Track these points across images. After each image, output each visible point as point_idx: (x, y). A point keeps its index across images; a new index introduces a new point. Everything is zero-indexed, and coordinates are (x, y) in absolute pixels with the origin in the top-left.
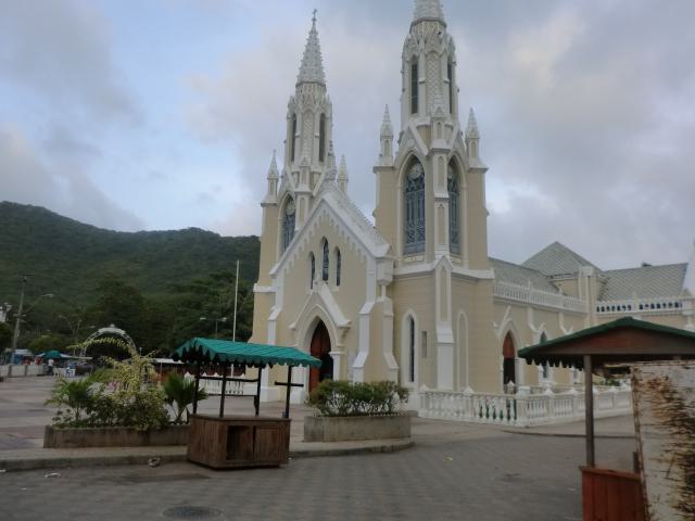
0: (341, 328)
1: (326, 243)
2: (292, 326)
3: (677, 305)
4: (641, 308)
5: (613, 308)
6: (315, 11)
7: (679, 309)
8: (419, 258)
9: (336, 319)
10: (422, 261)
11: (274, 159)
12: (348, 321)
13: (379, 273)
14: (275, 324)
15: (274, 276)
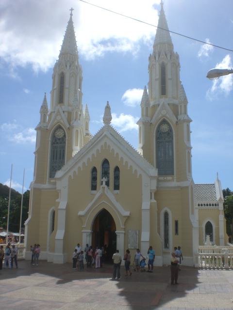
0: (125, 217)
1: (106, 162)
2: (81, 213)
3: (216, 205)
4: (199, 205)
5: (204, 204)
6: (72, 10)
7: (217, 207)
8: (169, 178)
9: (119, 211)
10: (173, 180)
11: (45, 96)
12: (129, 212)
13: (149, 186)
14: (64, 212)
15: (60, 179)
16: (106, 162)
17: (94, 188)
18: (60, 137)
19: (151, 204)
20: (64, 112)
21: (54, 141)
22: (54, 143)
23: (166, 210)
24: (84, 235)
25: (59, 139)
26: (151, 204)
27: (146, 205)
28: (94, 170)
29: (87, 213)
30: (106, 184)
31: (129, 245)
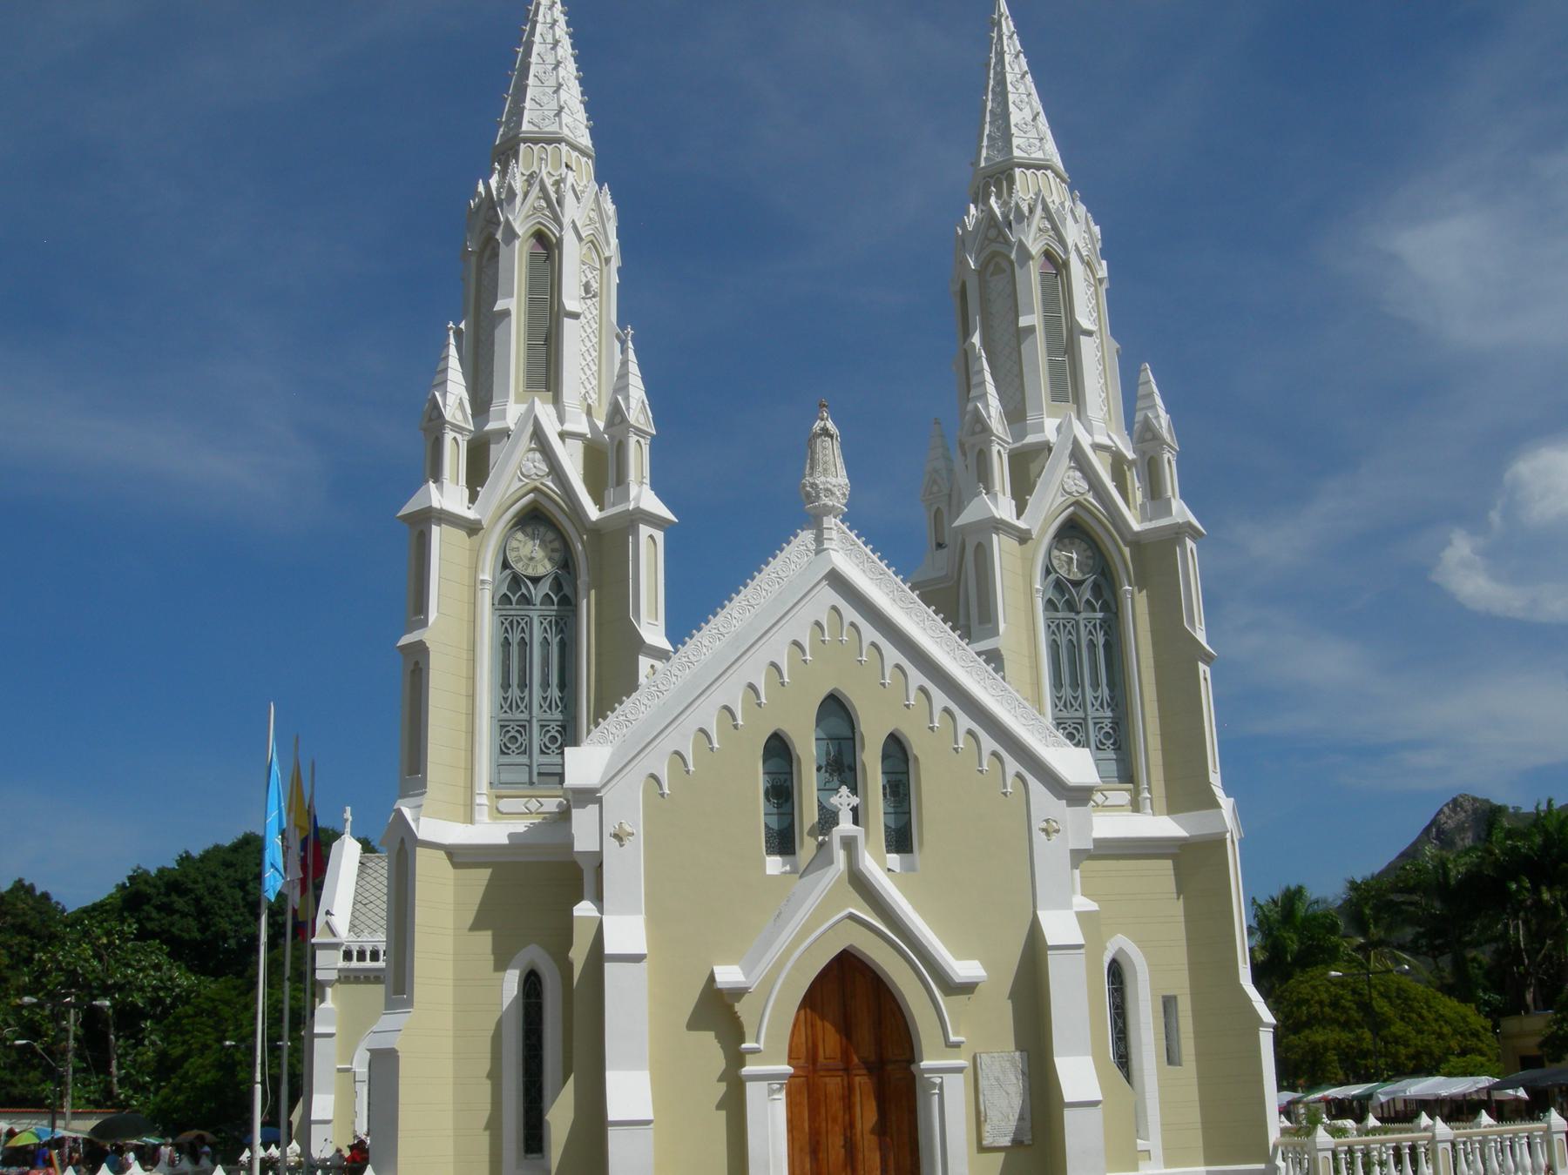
1: (835, 708)
2: (728, 975)
16: (835, 708)
17: (782, 841)
18: (541, 571)
19: (1083, 917)
20: (563, 436)
21: (504, 589)
22: (505, 599)
23: (1121, 950)
24: (754, 1092)
25: (536, 580)
26: (1080, 916)
27: (1059, 927)
28: (778, 749)
29: (768, 982)
30: (856, 822)
31: (987, 1128)
